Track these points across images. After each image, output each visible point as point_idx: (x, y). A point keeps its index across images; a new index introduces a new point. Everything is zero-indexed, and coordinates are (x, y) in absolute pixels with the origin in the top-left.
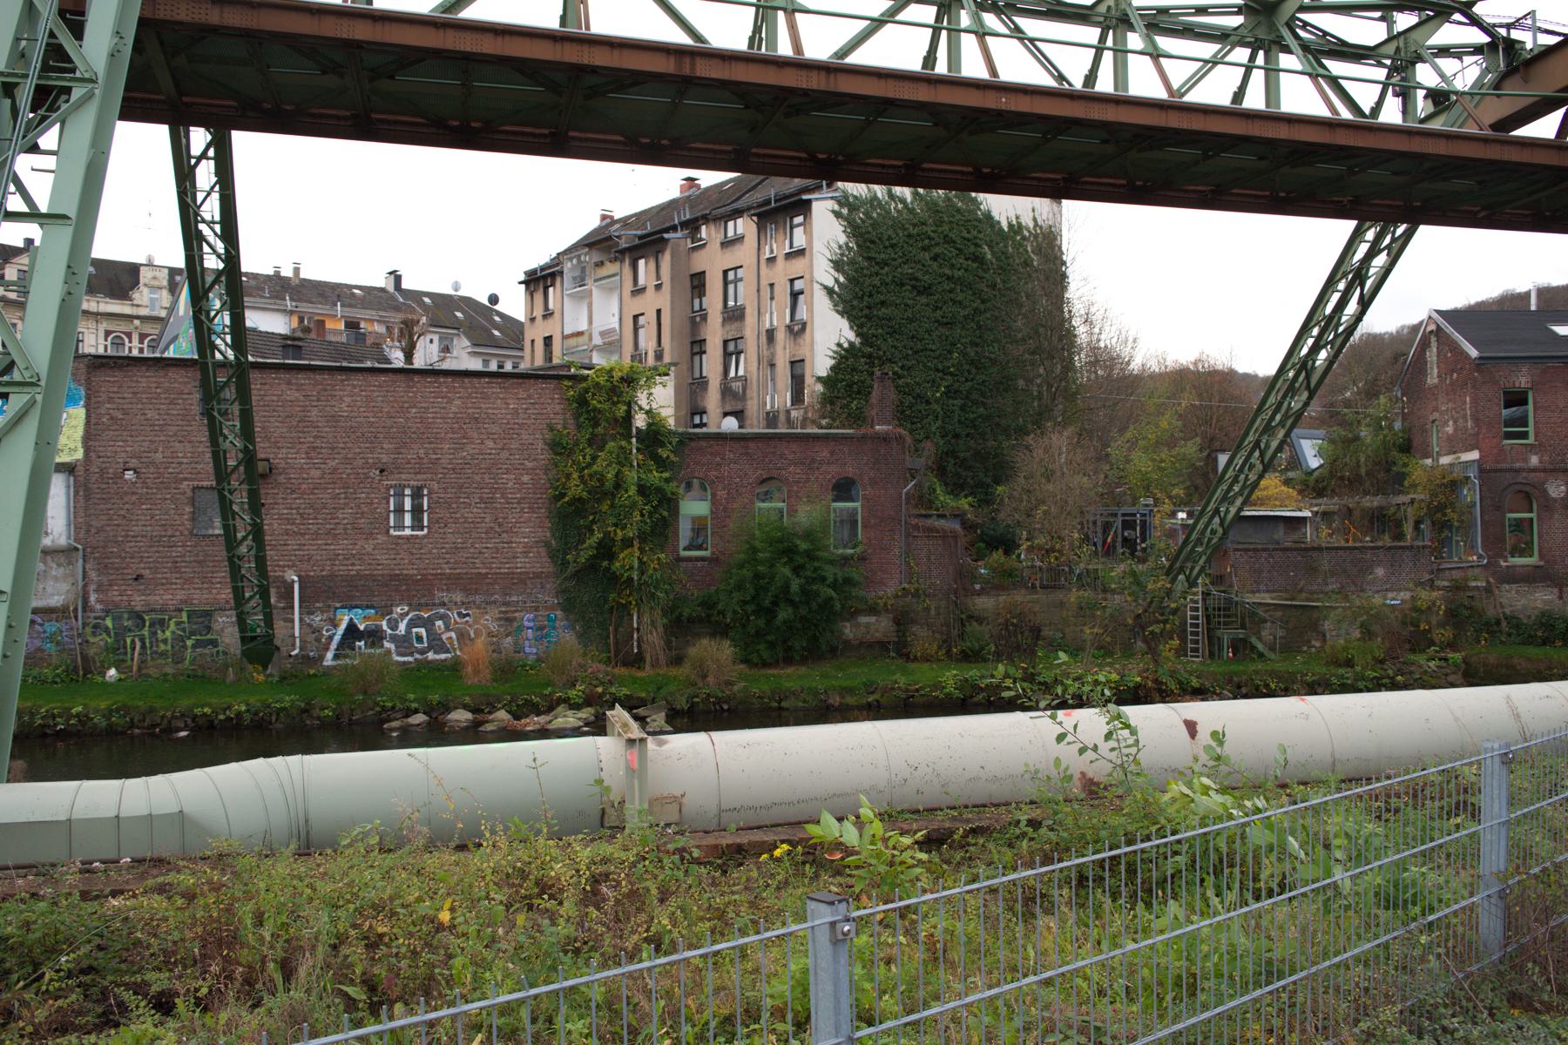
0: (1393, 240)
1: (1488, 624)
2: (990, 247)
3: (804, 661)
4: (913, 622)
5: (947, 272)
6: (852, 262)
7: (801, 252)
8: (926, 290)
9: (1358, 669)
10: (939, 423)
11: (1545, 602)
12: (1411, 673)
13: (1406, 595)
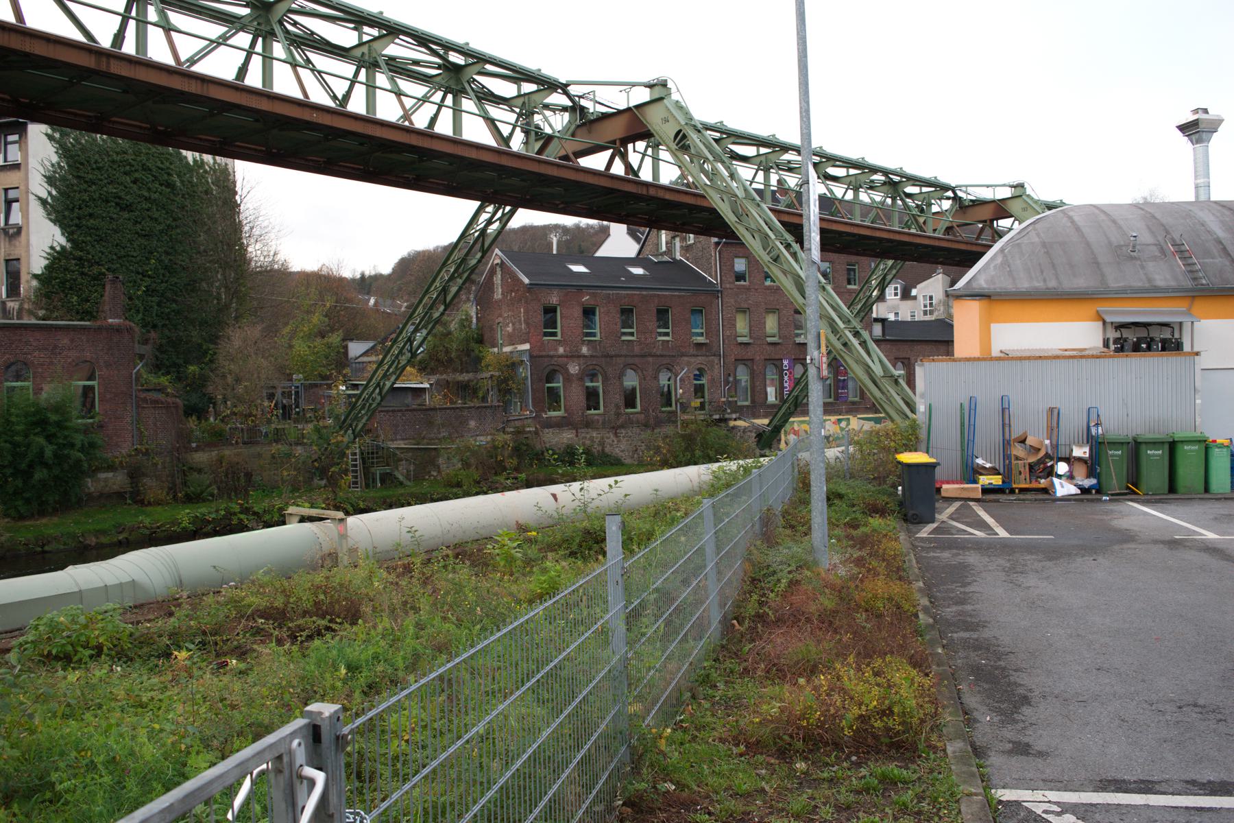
0: (503, 214)
1: (537, 454)
2: (179, 176)
3: (55, 511)
4: (144, 475)
5: (146, 194)
6: (63, 179)
7: (16, 167)
8: (128, 208)
10: (140, 316)
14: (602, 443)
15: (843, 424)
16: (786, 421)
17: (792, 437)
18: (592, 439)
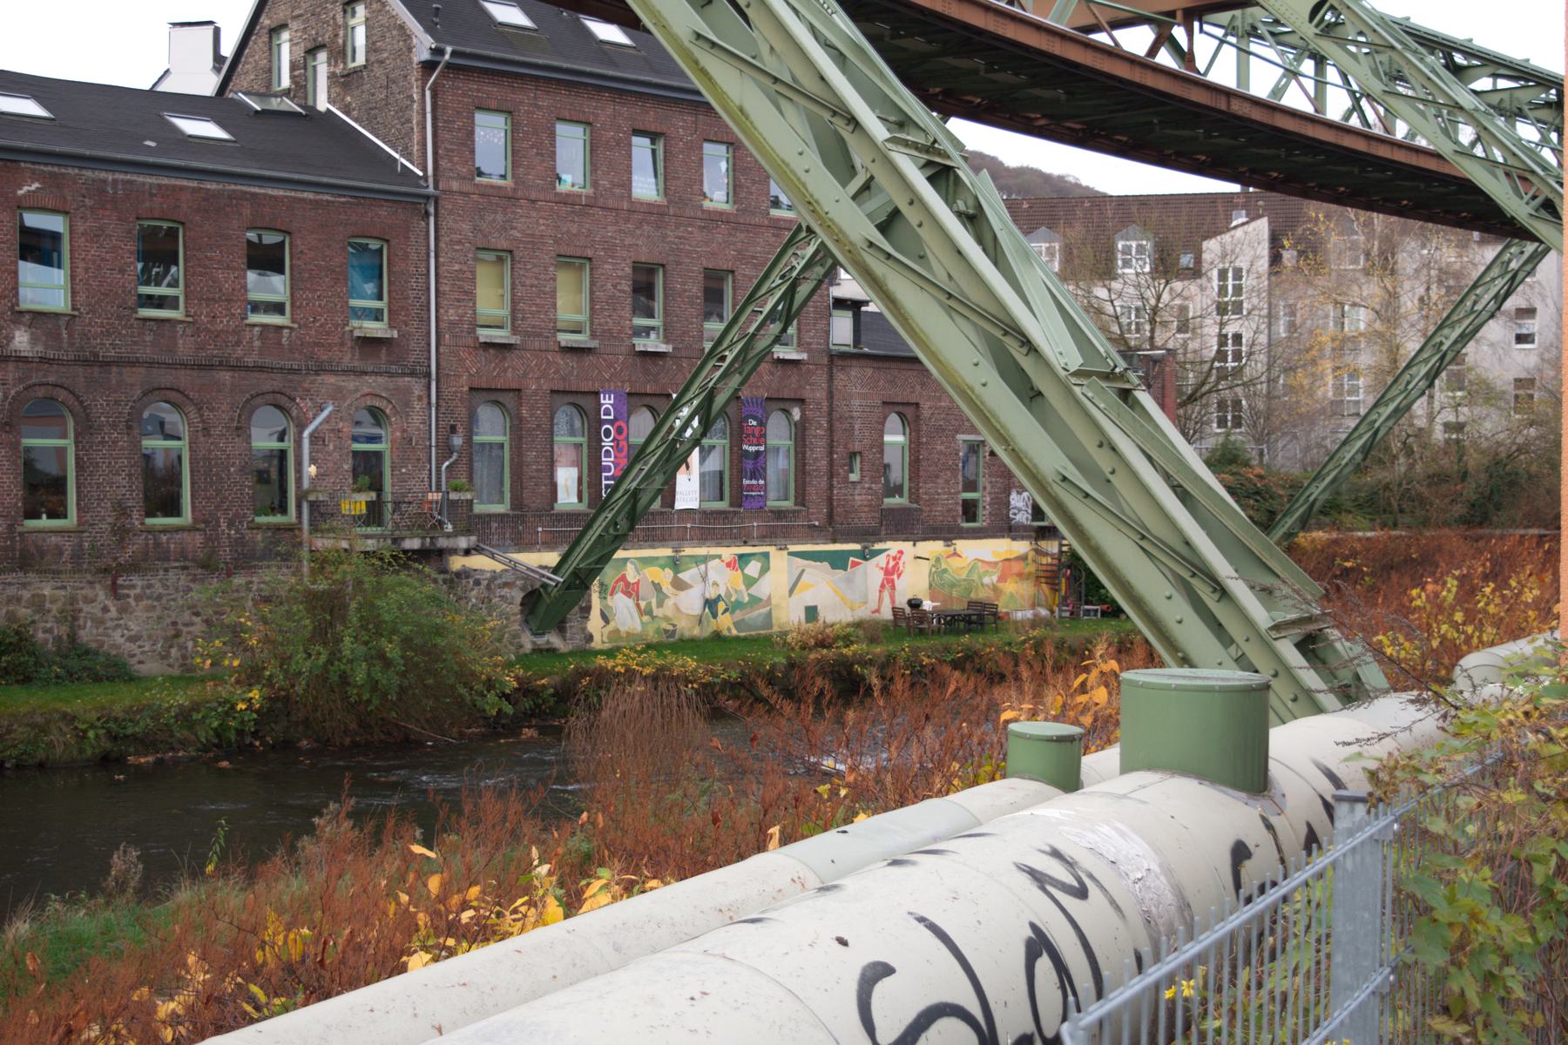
14: (71, 616)
15: (753, 568)
16: (605, 558)
17: (621, 604)
18: (38, 604)
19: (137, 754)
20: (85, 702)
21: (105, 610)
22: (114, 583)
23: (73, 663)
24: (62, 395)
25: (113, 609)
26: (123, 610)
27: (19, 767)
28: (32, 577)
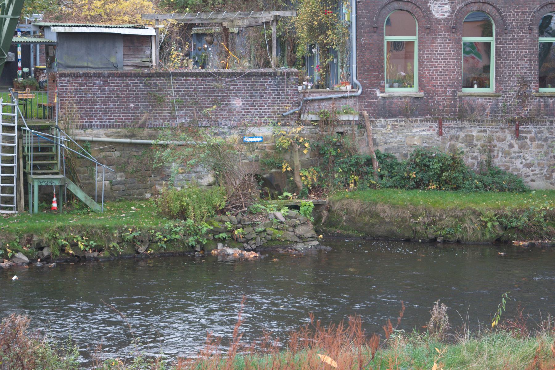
9: (190, 222)
11: (421, 137)
12: (254, 225)
13: (267, 131)
14: (489, 150)
19: (519, 239)
20: (489, 204)
21: (511, 146)
22: (517, 129)
23: (488, 179)
24: (488, 9)
25: (516, 146)
26: (522, 147)
27: (445, 242)
28: (466, 124)
